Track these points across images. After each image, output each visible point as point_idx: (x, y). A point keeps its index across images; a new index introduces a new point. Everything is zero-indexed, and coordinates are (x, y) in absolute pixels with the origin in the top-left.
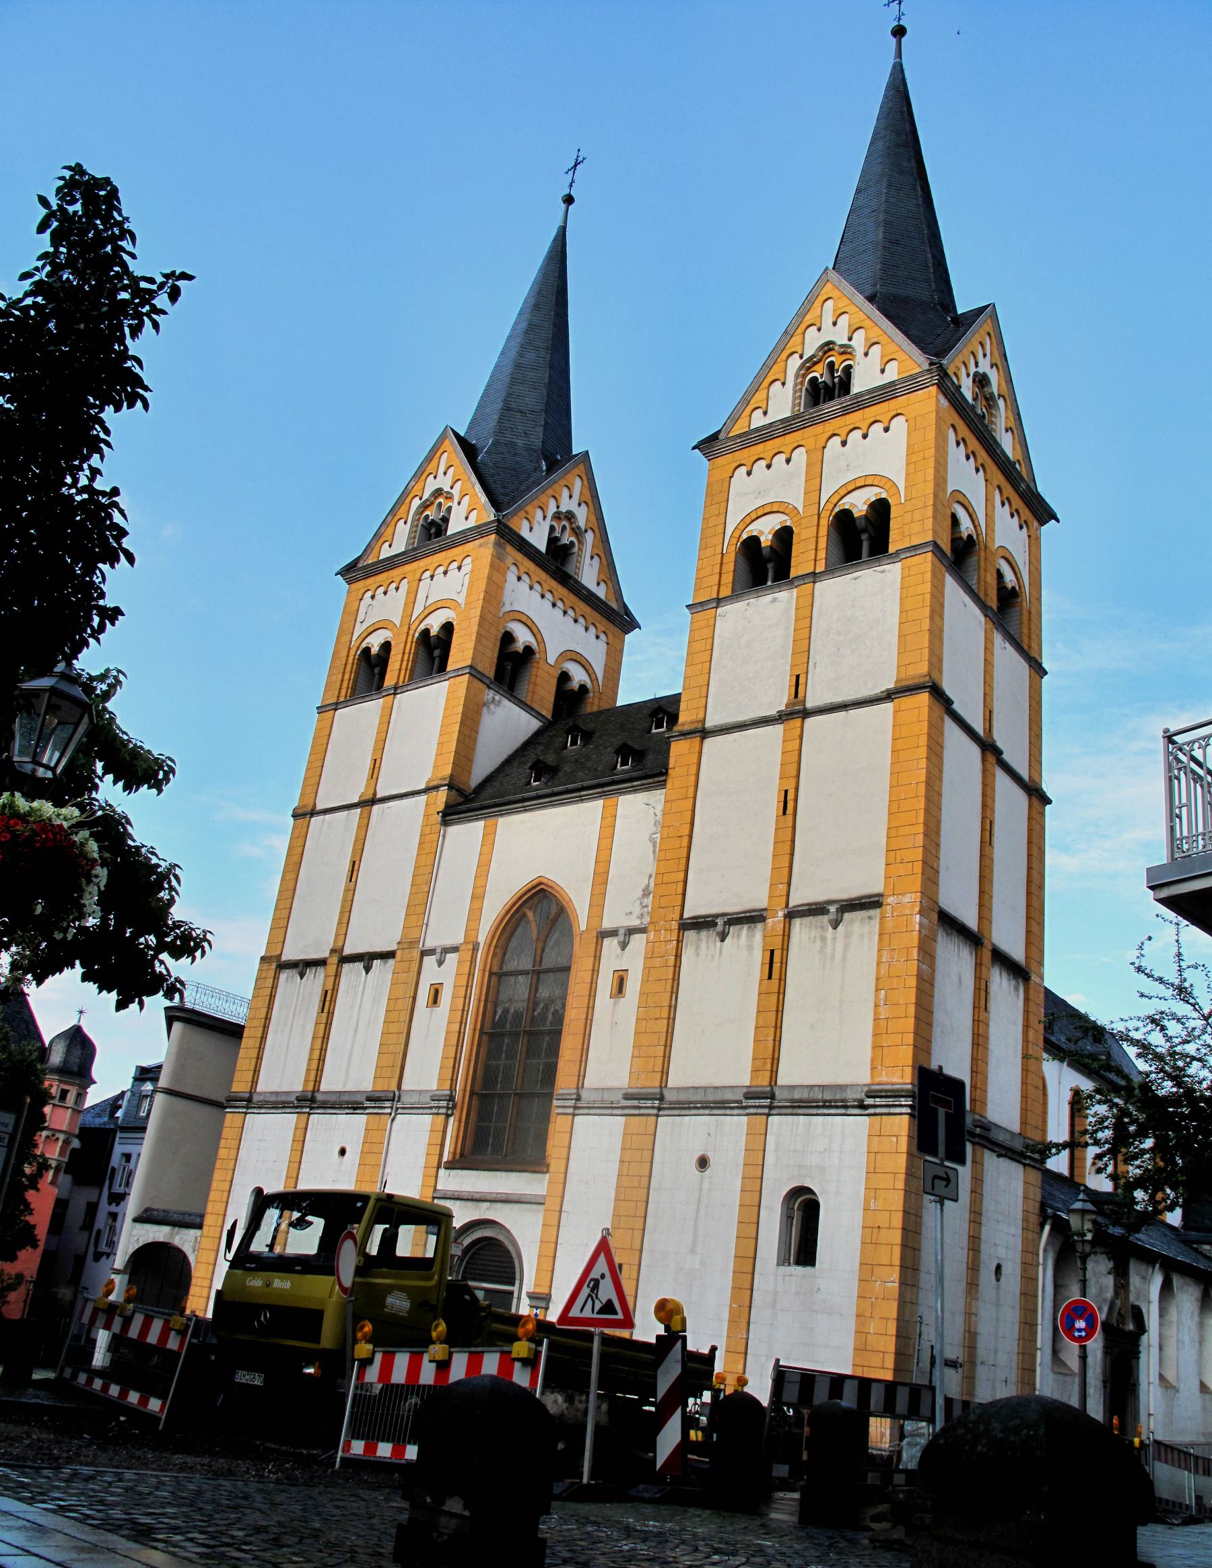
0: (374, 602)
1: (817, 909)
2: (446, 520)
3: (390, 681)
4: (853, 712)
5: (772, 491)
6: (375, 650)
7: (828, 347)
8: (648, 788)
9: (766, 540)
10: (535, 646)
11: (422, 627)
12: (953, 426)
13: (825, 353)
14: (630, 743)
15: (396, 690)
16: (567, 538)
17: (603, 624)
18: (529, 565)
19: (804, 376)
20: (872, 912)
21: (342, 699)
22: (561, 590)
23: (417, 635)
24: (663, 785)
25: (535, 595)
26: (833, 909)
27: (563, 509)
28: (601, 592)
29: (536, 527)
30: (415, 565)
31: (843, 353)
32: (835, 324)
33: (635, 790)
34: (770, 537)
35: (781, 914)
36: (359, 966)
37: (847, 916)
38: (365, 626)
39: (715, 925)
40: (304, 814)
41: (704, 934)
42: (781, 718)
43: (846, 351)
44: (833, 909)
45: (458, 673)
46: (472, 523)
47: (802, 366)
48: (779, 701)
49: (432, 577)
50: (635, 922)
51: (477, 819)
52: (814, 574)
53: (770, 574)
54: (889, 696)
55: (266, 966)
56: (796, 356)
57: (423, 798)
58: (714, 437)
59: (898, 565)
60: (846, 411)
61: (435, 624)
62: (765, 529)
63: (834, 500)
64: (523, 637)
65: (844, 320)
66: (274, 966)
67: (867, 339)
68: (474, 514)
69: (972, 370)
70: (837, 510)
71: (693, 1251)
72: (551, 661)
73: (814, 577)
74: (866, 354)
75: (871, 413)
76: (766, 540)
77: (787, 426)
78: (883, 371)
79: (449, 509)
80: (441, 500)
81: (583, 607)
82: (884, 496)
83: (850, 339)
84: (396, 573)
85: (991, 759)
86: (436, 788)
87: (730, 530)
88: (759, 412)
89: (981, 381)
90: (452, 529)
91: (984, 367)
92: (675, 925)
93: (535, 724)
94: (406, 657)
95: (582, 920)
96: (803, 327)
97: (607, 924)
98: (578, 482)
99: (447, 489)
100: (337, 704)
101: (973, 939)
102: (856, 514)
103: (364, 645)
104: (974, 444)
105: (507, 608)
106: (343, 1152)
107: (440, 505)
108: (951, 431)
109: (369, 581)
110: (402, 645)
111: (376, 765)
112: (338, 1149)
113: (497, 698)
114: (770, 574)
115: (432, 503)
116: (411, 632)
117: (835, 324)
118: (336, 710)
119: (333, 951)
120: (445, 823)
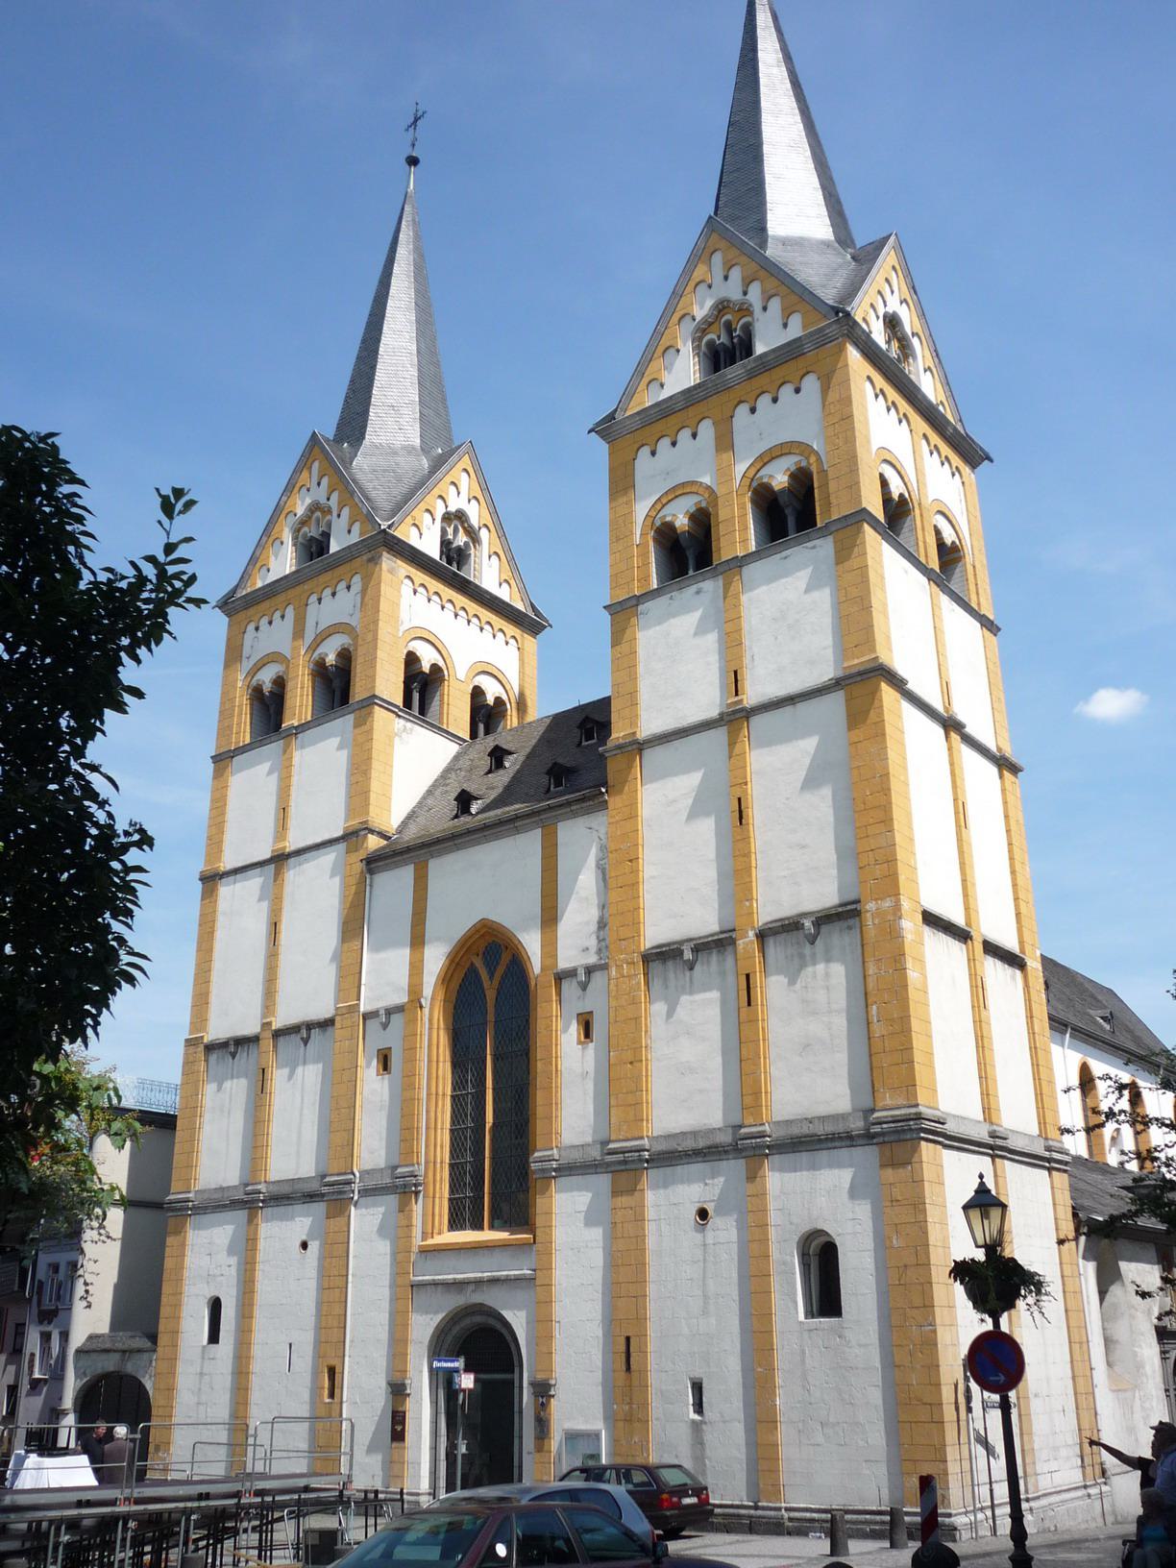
1: (789, 927)
2: (327, 535)
3: (290, 721)
6: (267, 688)
7: (722, 307)
8: (588, 812)
9: (682, 522)
10: (441, 663)
12: (869, 378)
14: (560, 761)
16: (461, 539)
17: (511, 630)
18: (420, 577)
19: (700, 339)
20: (851, 922)
22: (461, 600)
25: (435, 606)
26: (808, 924)
27: (452, 509)
28: (504, 594)
29: (424, 531)
30: (299, 589)
32: (726, 278)
33: (575, 815)
34: (686, 521)
35: (751, 934)
36: (295, 1039)
37: (824, 929)
39: (681, 953)
40: (211, 880)
41: (670, 964)
43: (745, 310)
44: (808, 924)
46: (355, 538)
49: (320, 600)
50: (592, 959)
53: (691, 563)
54: (836, 684)
55: (192, 1049)
56: (688, 319)
58: (611, 416)
59: (830, 539)
60: (751, 375)
63: (751, 474)
64: (428, 657)
65: (736, 274)
66: (201, 1048)
67: (763, 292)
68: (356, 527)
69: (881, 311)
71: (705, 1312)
72: (461, 674)
74: (765, 309)
75: (778, 374)
76: (682, 522)
77: (690, 398)
78: (785, 325)
79: (329, 524)
81: (486, 615)
82: (804, 464)
83: (745, 293)
84: (281, 598)
85: (955, 737)
88: (654, 386)
89: (892, 322)
90: (334, 547)
91: (894, 305)
92: (637, 958)
93: (453, 748)
95: (536, 964)
96: (692, 284)
97: (564, 963)
98: (464, 481)
99: (323, 501)
101: (962, 935)
104: (892, 394)
105: (406, 626)
106: (304, 1245)
107: (318, 520)
108: (868, 385)
109: (252, 611)
112: (298, 1244)
113: (409, 725)
114: (691, 563)
117: (726, 278)
119: (266, 1025)
120: (371, 872)
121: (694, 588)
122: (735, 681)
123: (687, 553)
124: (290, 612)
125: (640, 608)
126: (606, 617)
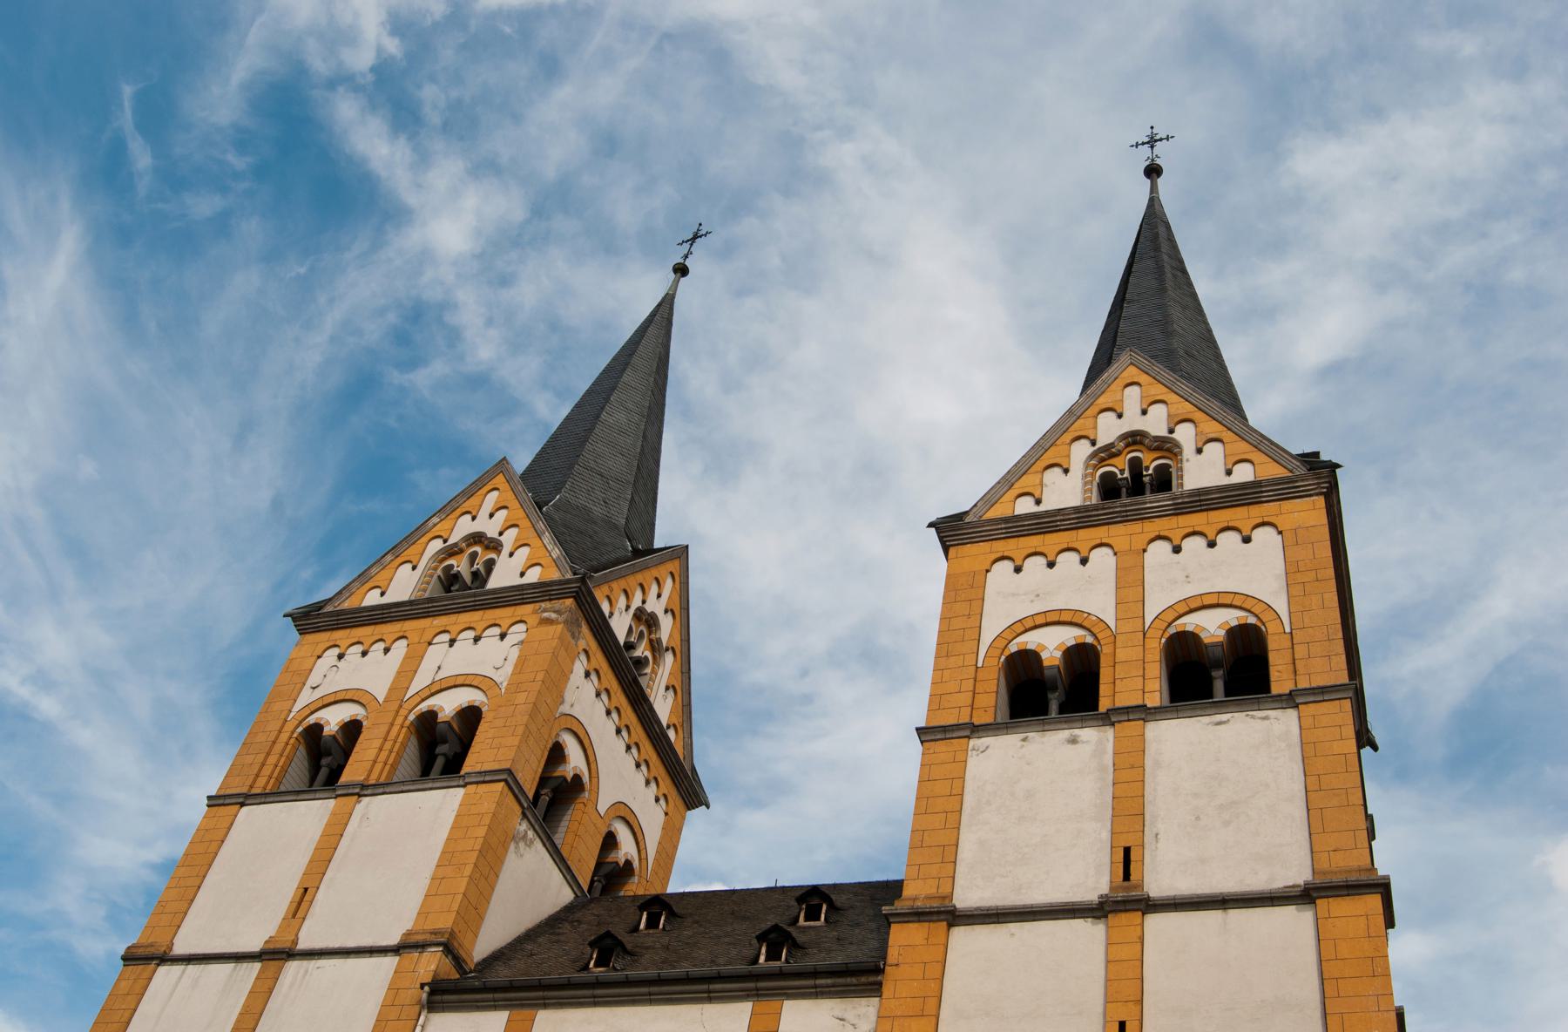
0: (342, 664)
4: (1236, 916)
5: (1049, 597)
11: (424, 706)
13: (1127, 446)
15: (364, 789)
21: (254, 791)
23: (412, 717)
24: (875, 989)
31: (1157, 449)
34: (1058, 654)
38: (318, 694)
42: (1099, 910)
45: (485, 777)
47: (1093, 455)
48: (1094, 883)
51: (495, 1008)
52: (1142, 708)
57: (390, 962)
61: (448, 705)
62: (1051, 644)
70: (1172, 630)
73: (1144, 713)
80: (478, 549)
86: (421, 946)
87: (987, 638)
94: (388, 745)
100: (247, 796)
102: (1206, 638)
103: (312, 720)
109: (338, 635)
110: (384, 729)
111: (304, 897)
115: (461, 551)
116: (403, 712)
118: (242, 805)
121: (1065, 734)
122: (1127, 861)
123: (1050, 691)
124: (400, 648)
125: (973, 742)
126: (915, 747)
